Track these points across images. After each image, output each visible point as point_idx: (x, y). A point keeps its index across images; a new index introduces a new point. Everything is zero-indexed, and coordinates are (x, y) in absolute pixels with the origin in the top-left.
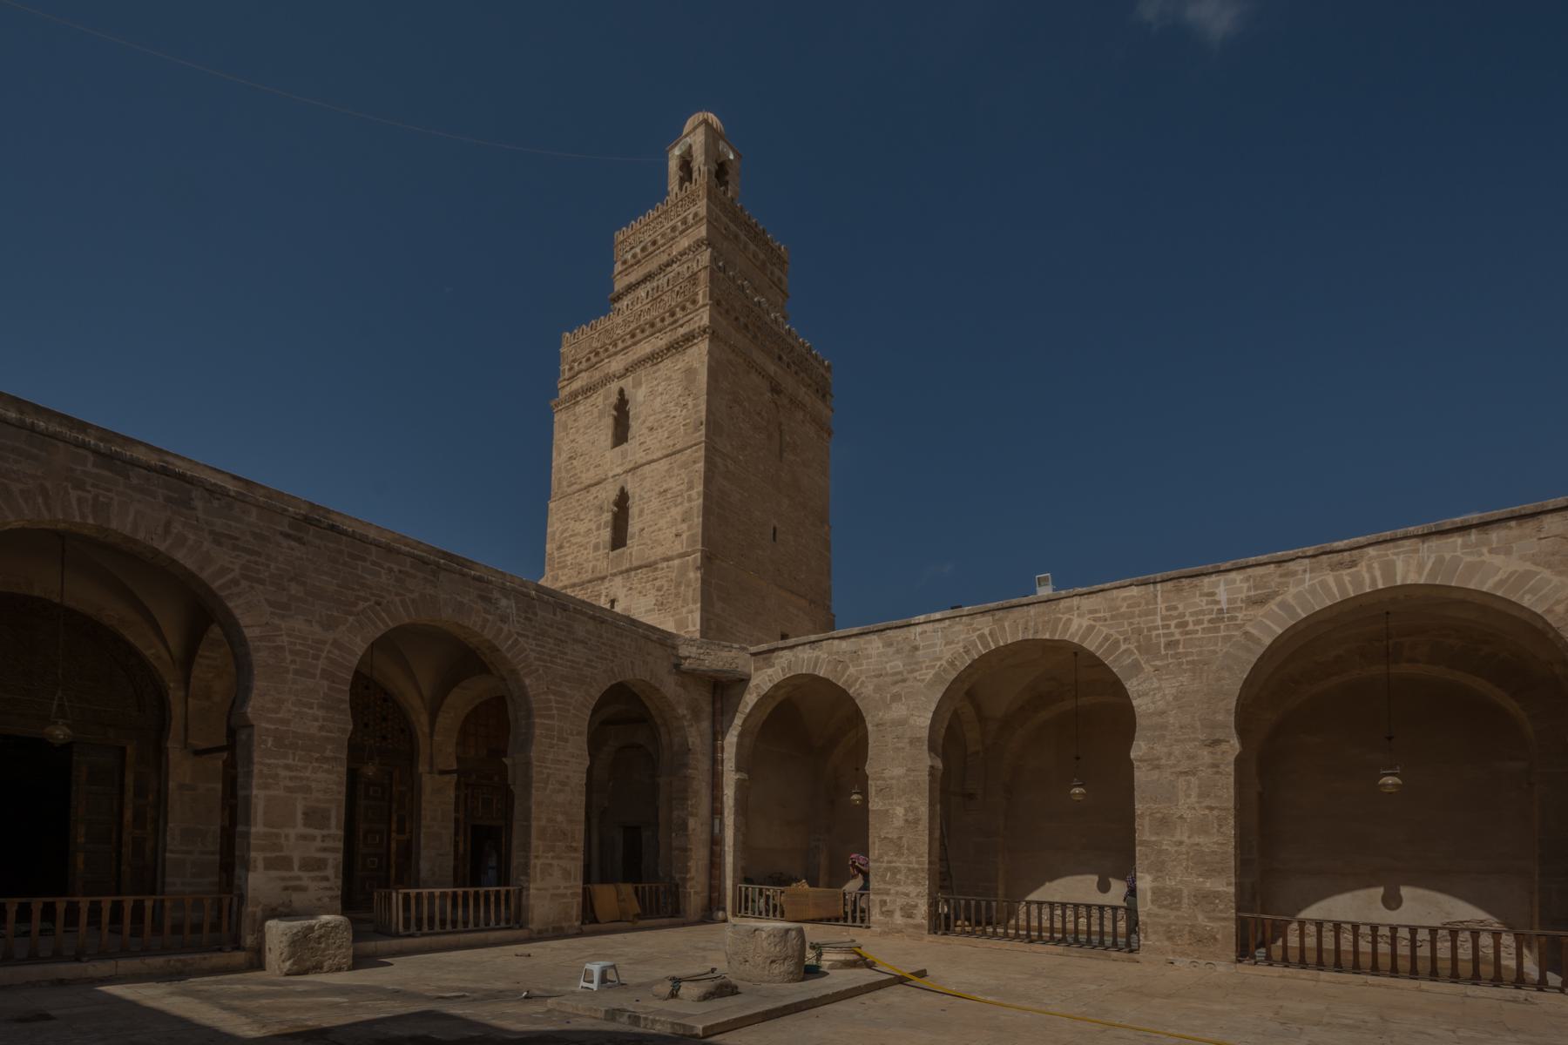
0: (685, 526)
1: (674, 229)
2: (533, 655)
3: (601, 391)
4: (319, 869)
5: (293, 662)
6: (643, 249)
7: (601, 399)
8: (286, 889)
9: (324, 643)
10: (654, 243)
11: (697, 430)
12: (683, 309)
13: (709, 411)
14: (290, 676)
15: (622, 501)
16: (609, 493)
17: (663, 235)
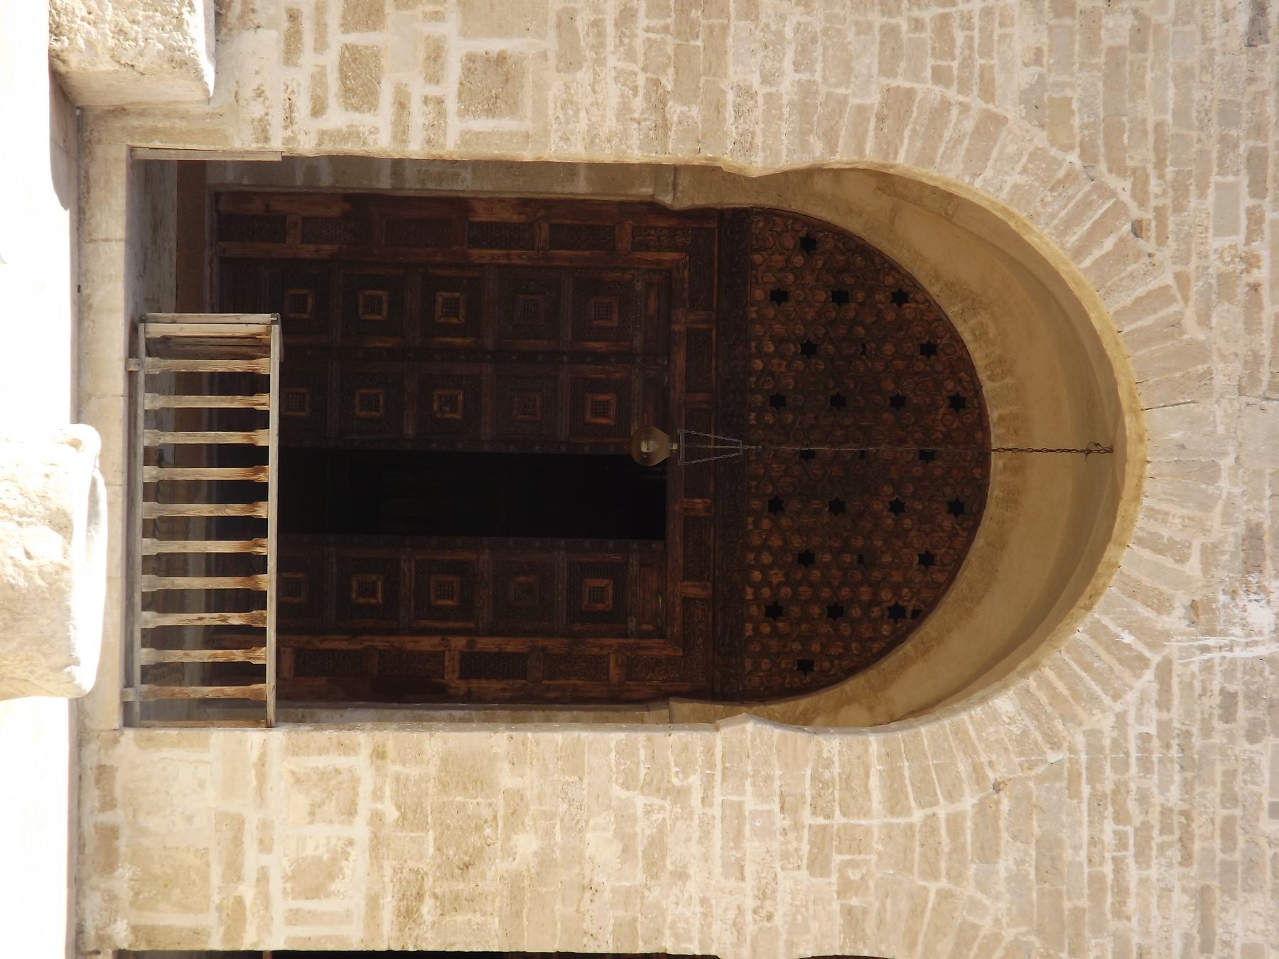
2: (1106, 723)
4: (347, 92)
5: (918, 25)
8: (293, 16)
9: (988, 92)
14: (877, 19)
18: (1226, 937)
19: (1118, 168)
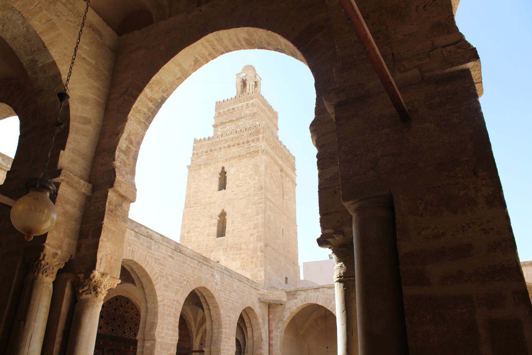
0: (255, 231)
2: (223, 299)
6: (228, 110)
10: (233, 109)
15: (223, 215)
19: (183, 283)
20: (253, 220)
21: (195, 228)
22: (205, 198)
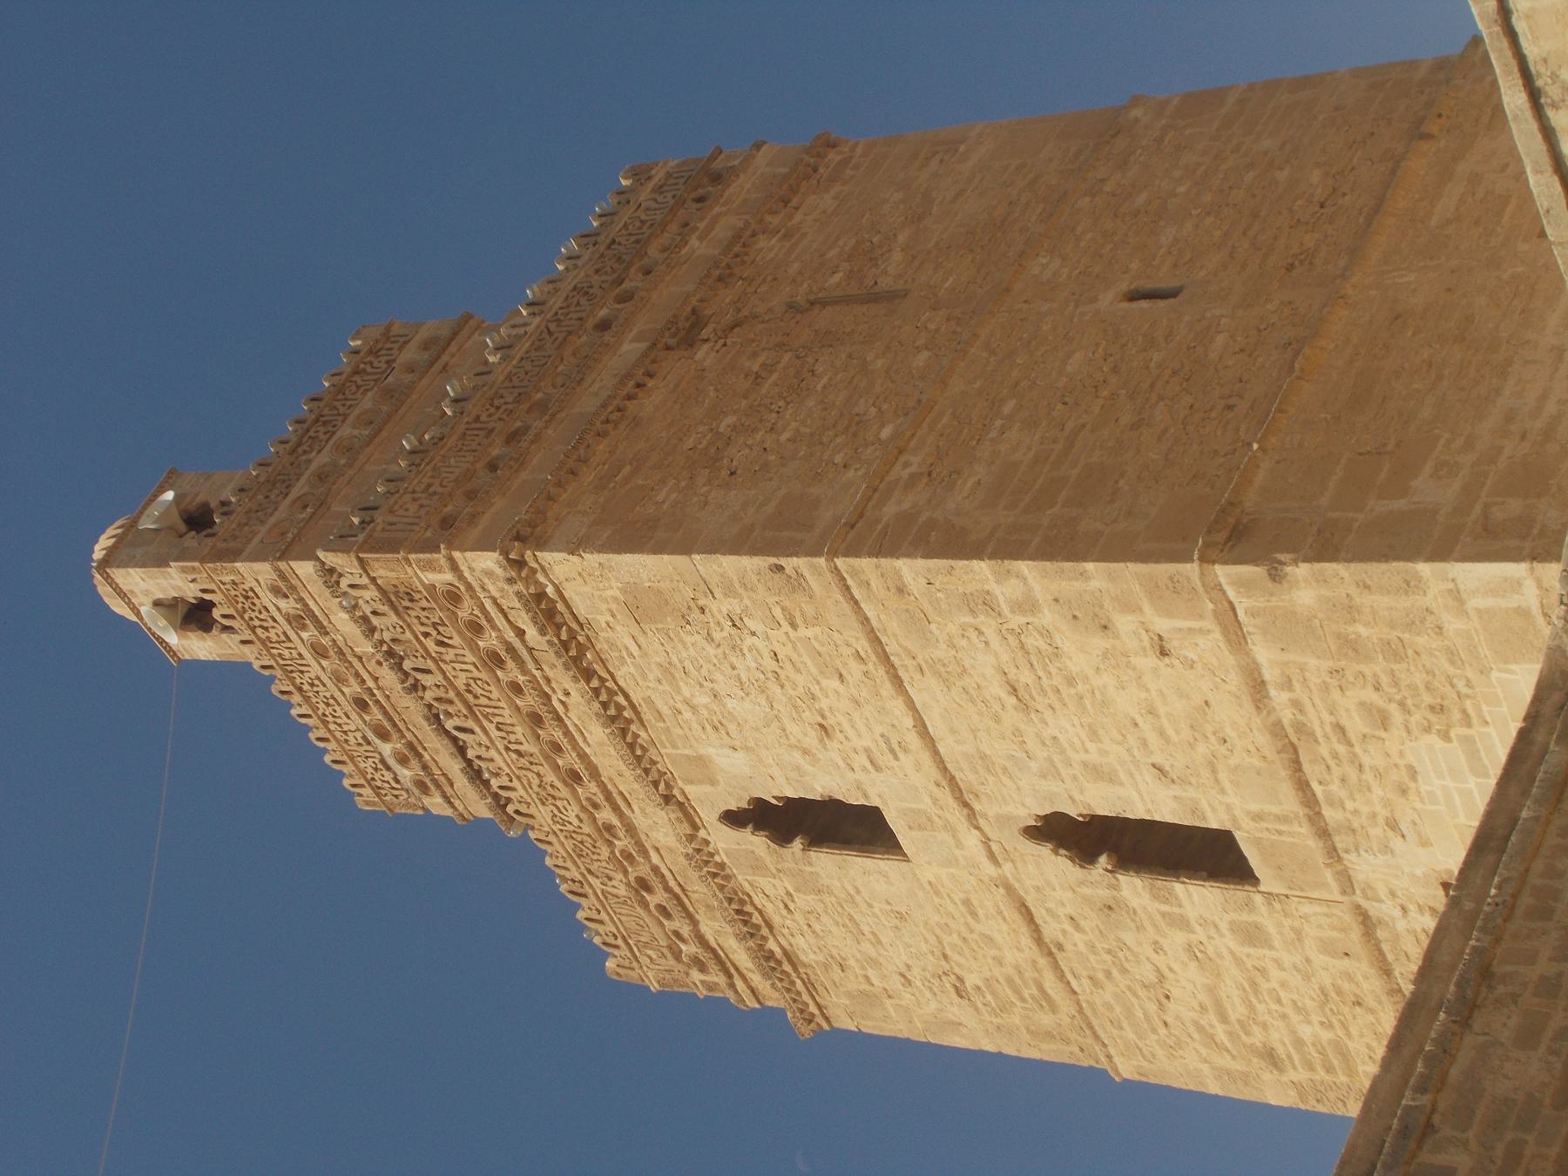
0: (1125, 623)
1: (320, 652)
3: (743, 879)
6: (384, 736)
7: (763, 882)
10: (361, 705)
11: (797, 583)
12: (476, 628)
13: (736, 546)
16: (1050, 870)
17: (339, 680)
18: (1553, 1059)
20: (1046, 633)
21: (1224, 1018)
22: (989, 939)
